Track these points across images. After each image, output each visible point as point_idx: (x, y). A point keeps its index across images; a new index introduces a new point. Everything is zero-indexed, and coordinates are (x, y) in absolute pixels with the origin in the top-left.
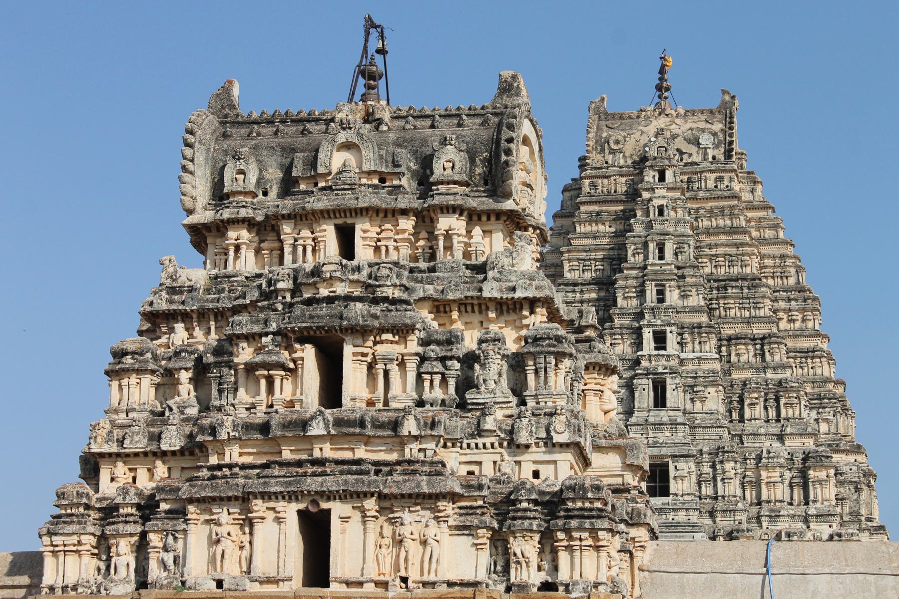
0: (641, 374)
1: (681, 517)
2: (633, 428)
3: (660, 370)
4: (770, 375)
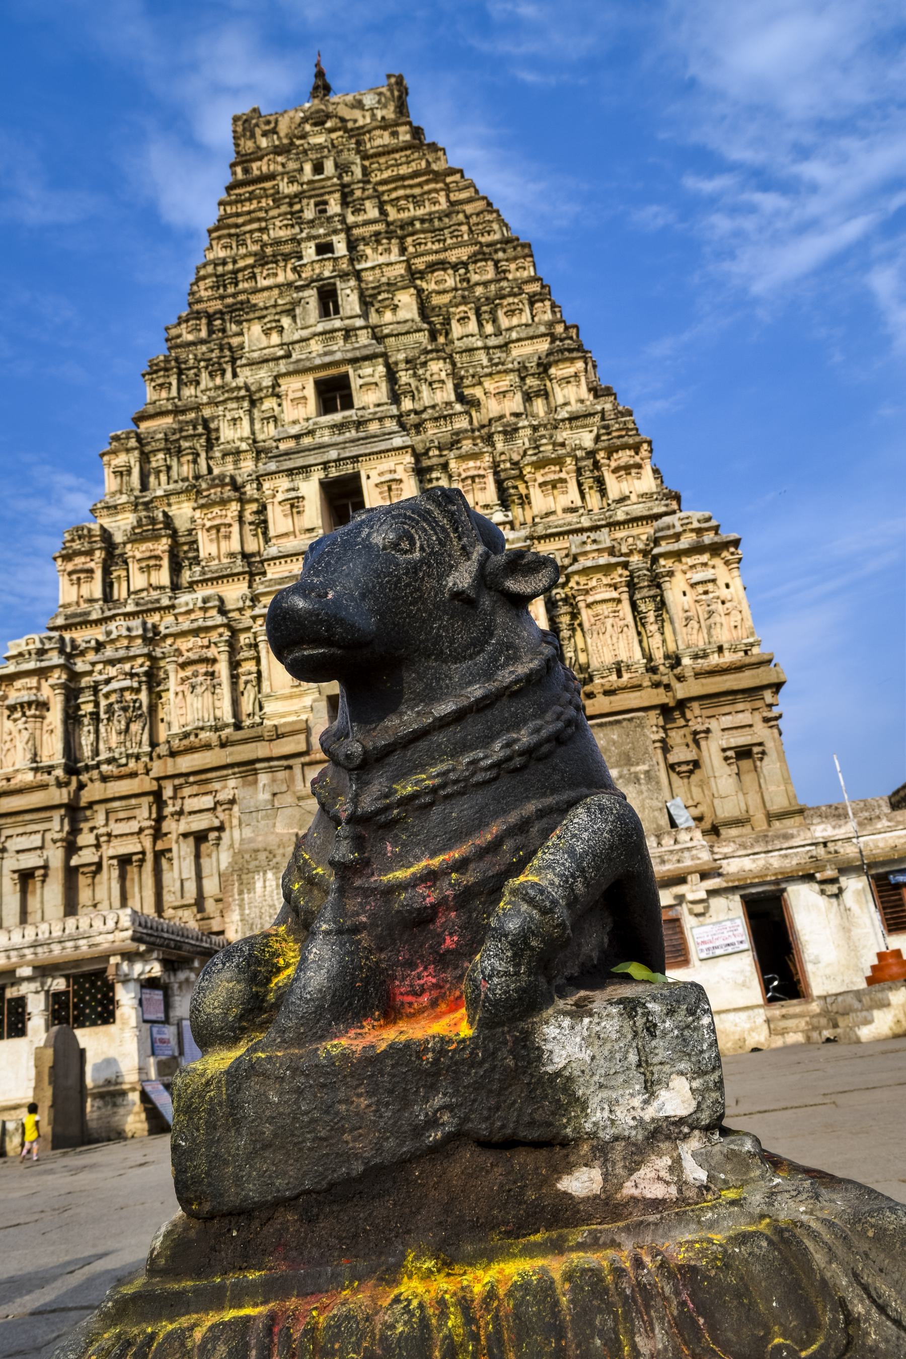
0: (302, 286)
1: (374, 427)
2: (297, 346)
3: (327, 274)
4: (479, 291)
